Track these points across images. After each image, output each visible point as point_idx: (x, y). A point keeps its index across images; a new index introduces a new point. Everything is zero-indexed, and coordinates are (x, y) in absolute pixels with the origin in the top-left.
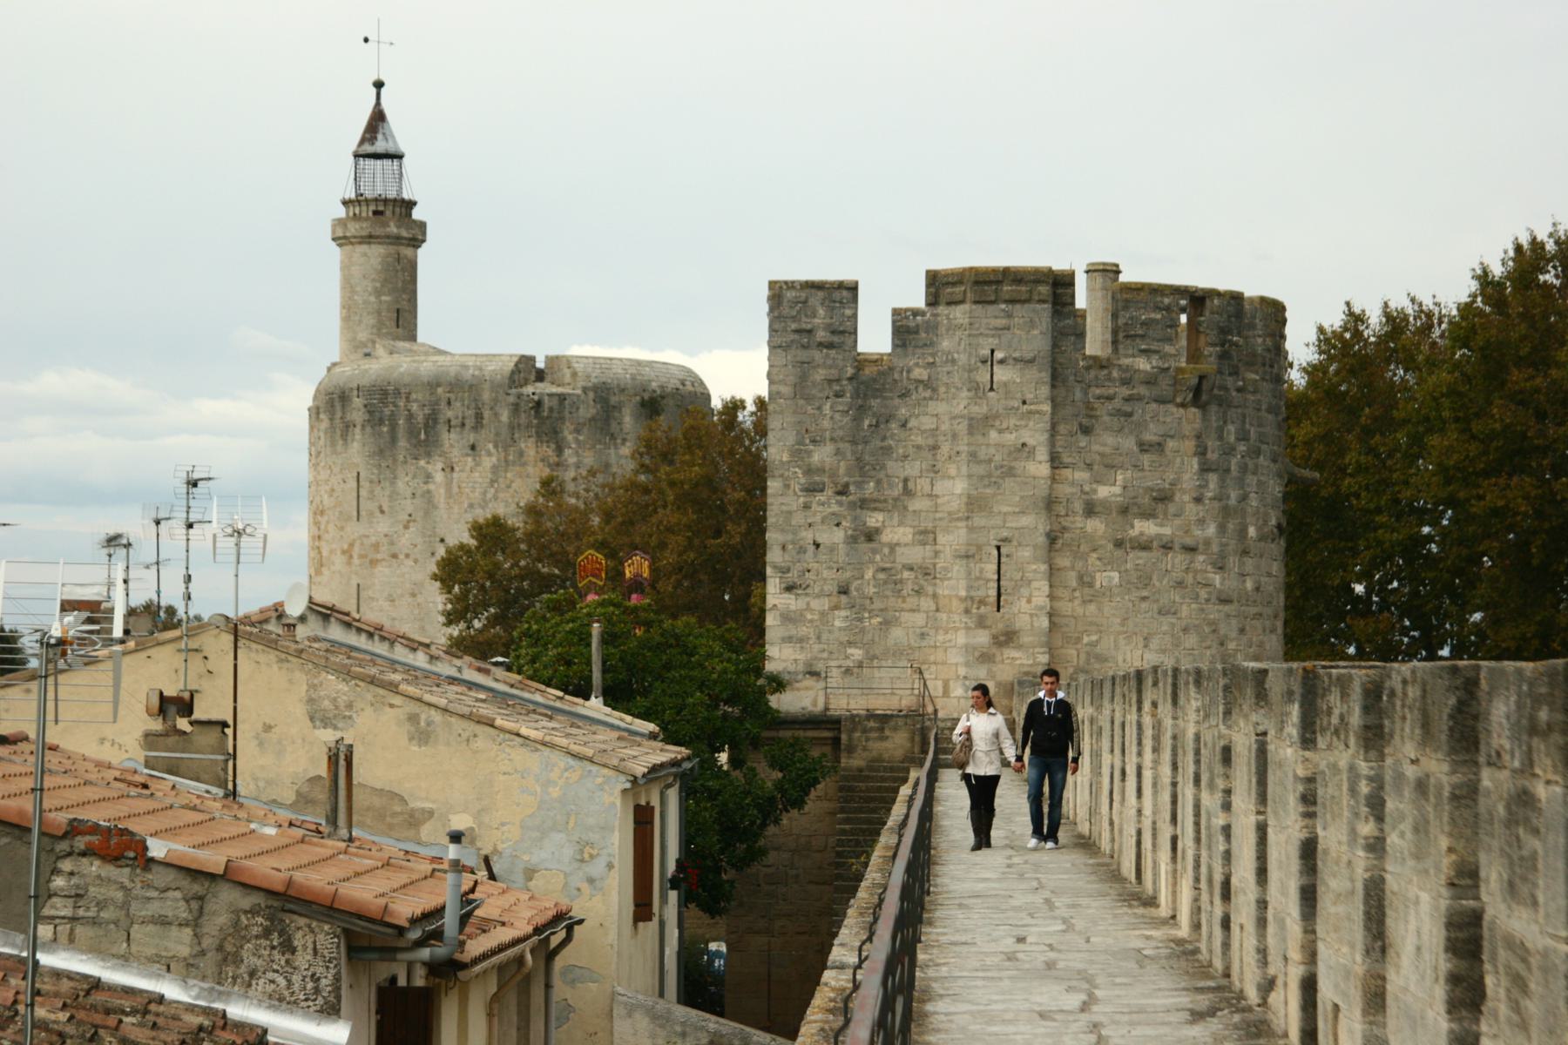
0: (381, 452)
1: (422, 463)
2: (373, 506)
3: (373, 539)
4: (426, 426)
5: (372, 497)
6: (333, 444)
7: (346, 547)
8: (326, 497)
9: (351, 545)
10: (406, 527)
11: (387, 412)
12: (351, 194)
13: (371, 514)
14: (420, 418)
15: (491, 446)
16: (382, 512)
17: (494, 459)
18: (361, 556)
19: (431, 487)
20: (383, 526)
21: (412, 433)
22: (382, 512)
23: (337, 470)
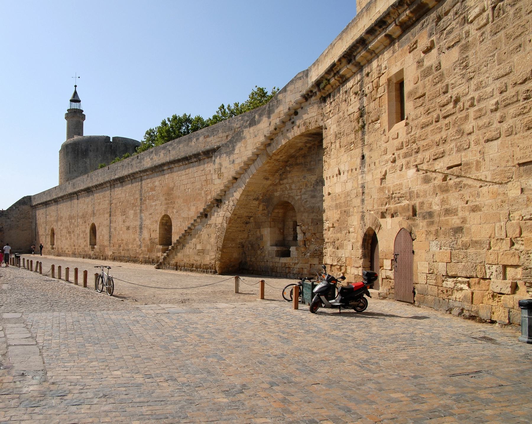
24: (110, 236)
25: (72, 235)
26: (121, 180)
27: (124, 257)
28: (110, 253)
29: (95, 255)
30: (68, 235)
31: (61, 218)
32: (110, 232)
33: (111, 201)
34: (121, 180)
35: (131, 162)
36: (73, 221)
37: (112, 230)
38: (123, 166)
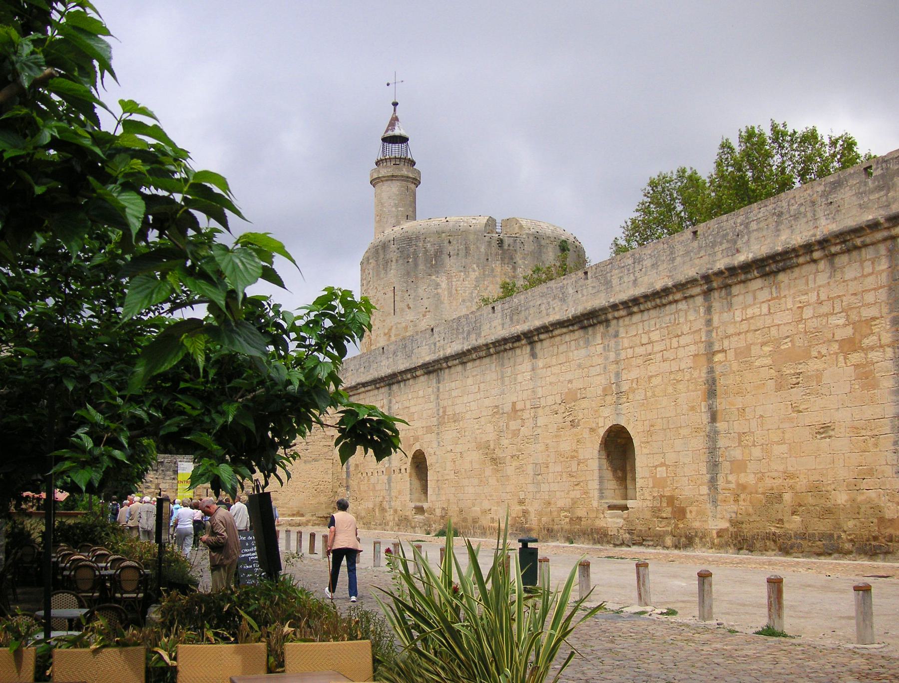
0: (408, 273)
1: (434, 277)
2: (404, 305)
3: (404, 325)
6: (378, 275)
7: (386, 331)
10: (424, 316)
11: (412, 250)
12: (380, 157)
13: (402, 310)
15: (475, 266)
16: (409, 308)
18: (396, 335)
19: (440, 291)
20: (410, 316)
21: (428, 260)
22: (409, 308)
24: (714, 466)
25: (510, 470)
26: (771, 266)
27: (803, 536)
28: (716, 523)
29: (630, 532)
30: (488, 471)
31: (456, 418)
32: (713, 450)
33: (710, 344)
34: (771, 266)
35: (825, 195)
36: (514, 425)
37: (722, 443)
38: (780, 214)
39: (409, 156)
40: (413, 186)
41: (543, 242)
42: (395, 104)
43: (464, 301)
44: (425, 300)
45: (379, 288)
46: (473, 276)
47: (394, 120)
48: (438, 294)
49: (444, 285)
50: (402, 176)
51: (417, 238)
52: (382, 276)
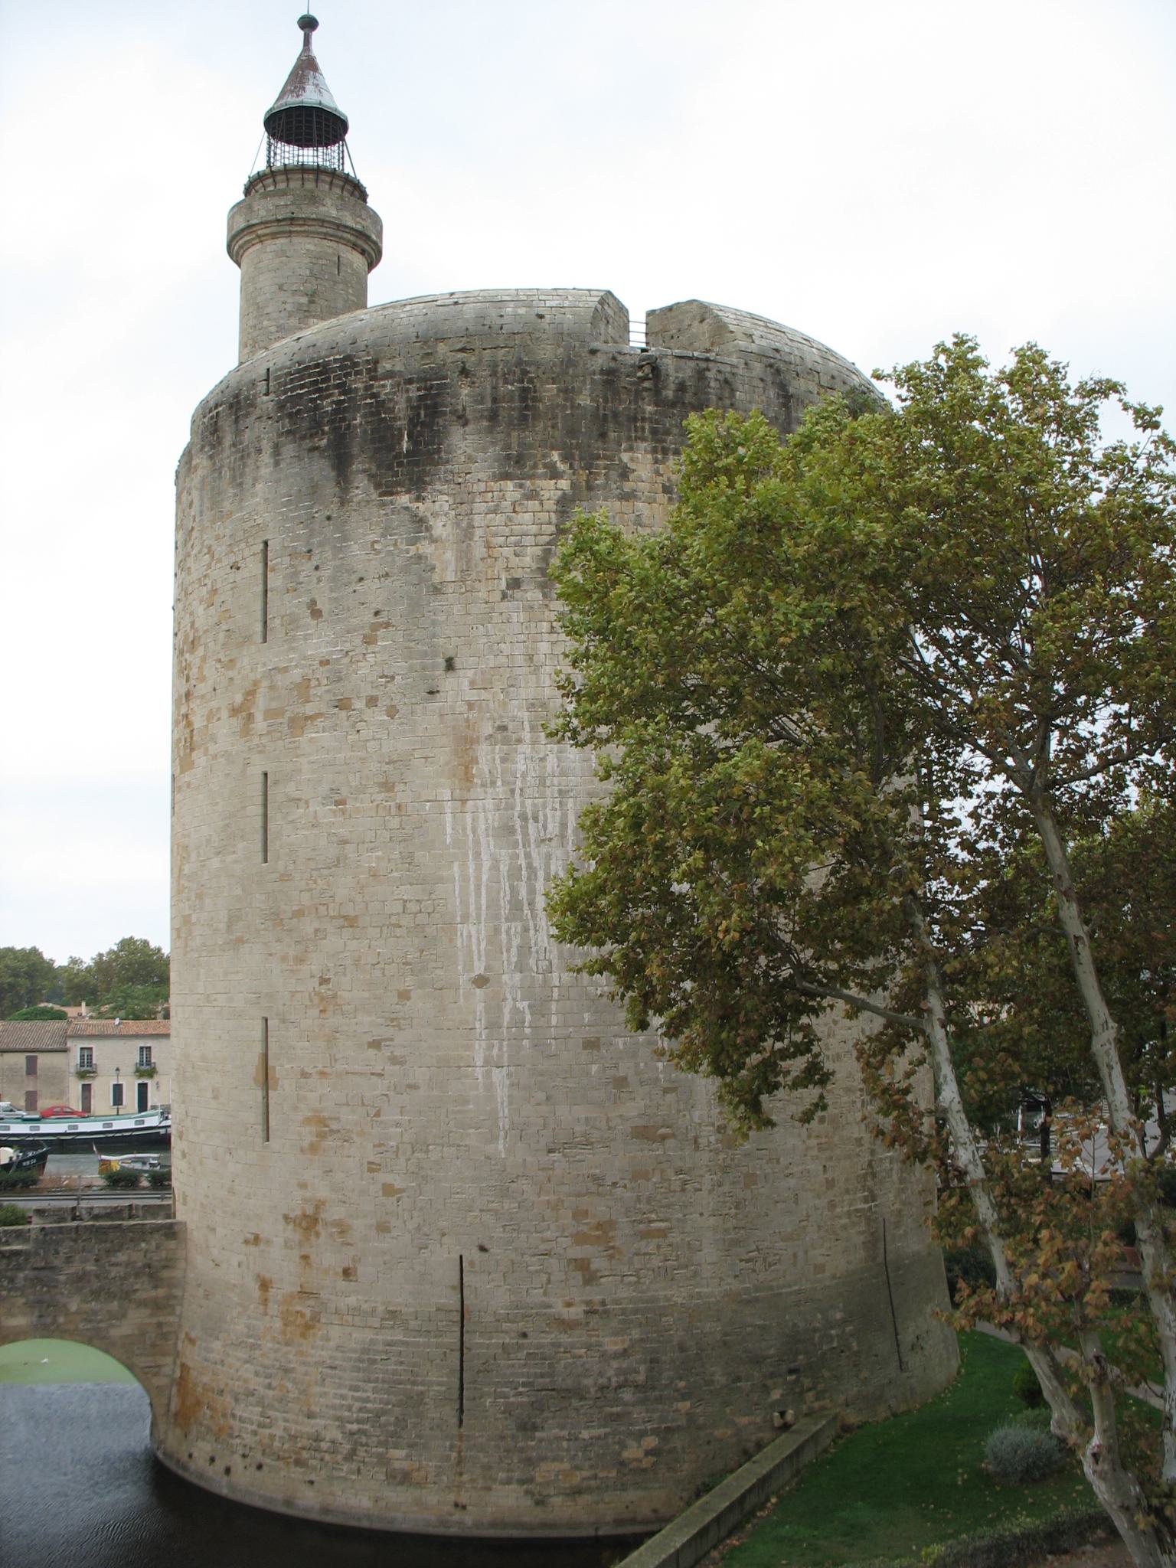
2: (295, 605)
3: (296, 674)
4: (413, 422)
5: (294, 585)
6: (215, 504)
7: (239, 699)
8: (200, 611)
9: (251, 694)
10: (369, 640)
11: (327, 405)
12: (262, 166)
13: (292, 622)
14: (401, 406)
15: (555, 456)
16: (316, 613)
17: (564, 484)
18: (269, 714)
19: (425, 548)
20: (319, 642)
21: (382, 437)
22: (316, 613)
23: (220, 550)
39: (348, 169)
40: (358, 260)
41: (797, 386)
42: (308, 24)
43: (515, 584)
44: (372, 584)
45: (220, 550)
46: (551, 490)
47: (306, 66)
48: (419, 558)
49: (441, 528)
50: (322, 222)
51: (349, 363)
52: (227, 506)
